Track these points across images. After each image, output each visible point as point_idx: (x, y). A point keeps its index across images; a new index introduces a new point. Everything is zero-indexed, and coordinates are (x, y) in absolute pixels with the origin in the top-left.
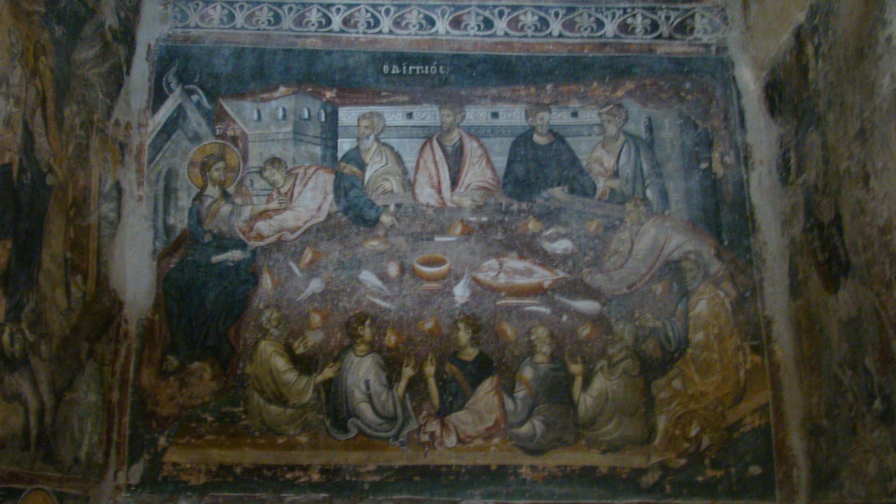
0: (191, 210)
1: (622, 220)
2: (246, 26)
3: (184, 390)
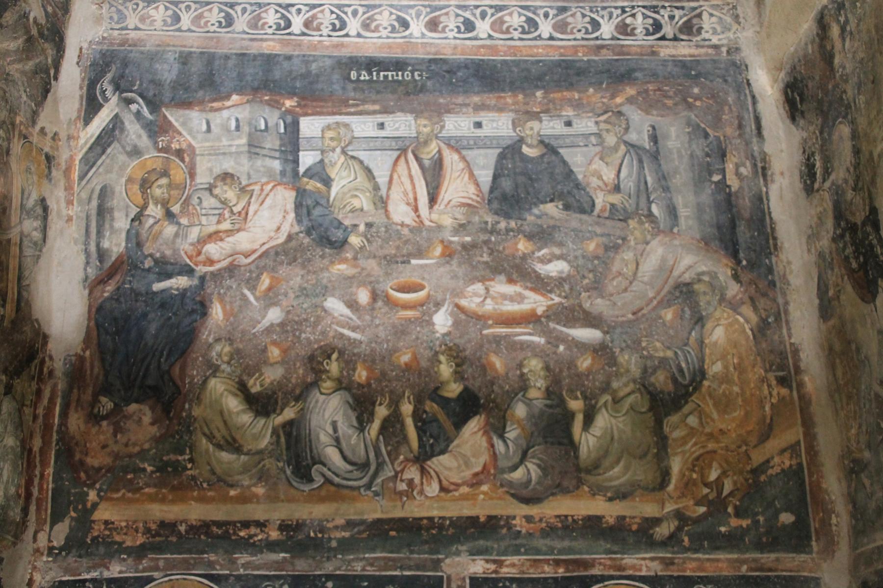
0: (128, 231)
1: (624, 239)
2: (193, 28)
3: (119, 436)
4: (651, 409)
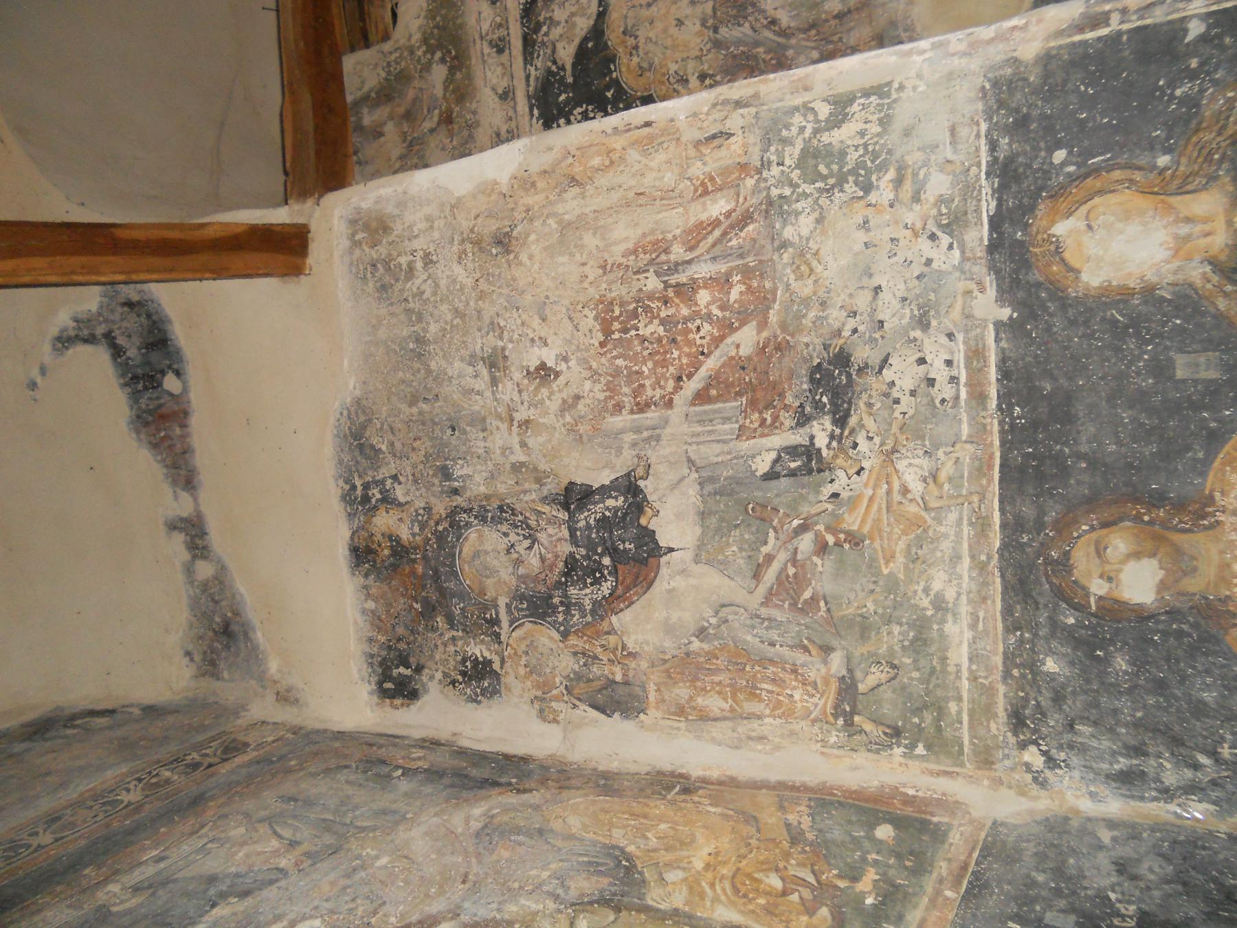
4: (618, 909)
